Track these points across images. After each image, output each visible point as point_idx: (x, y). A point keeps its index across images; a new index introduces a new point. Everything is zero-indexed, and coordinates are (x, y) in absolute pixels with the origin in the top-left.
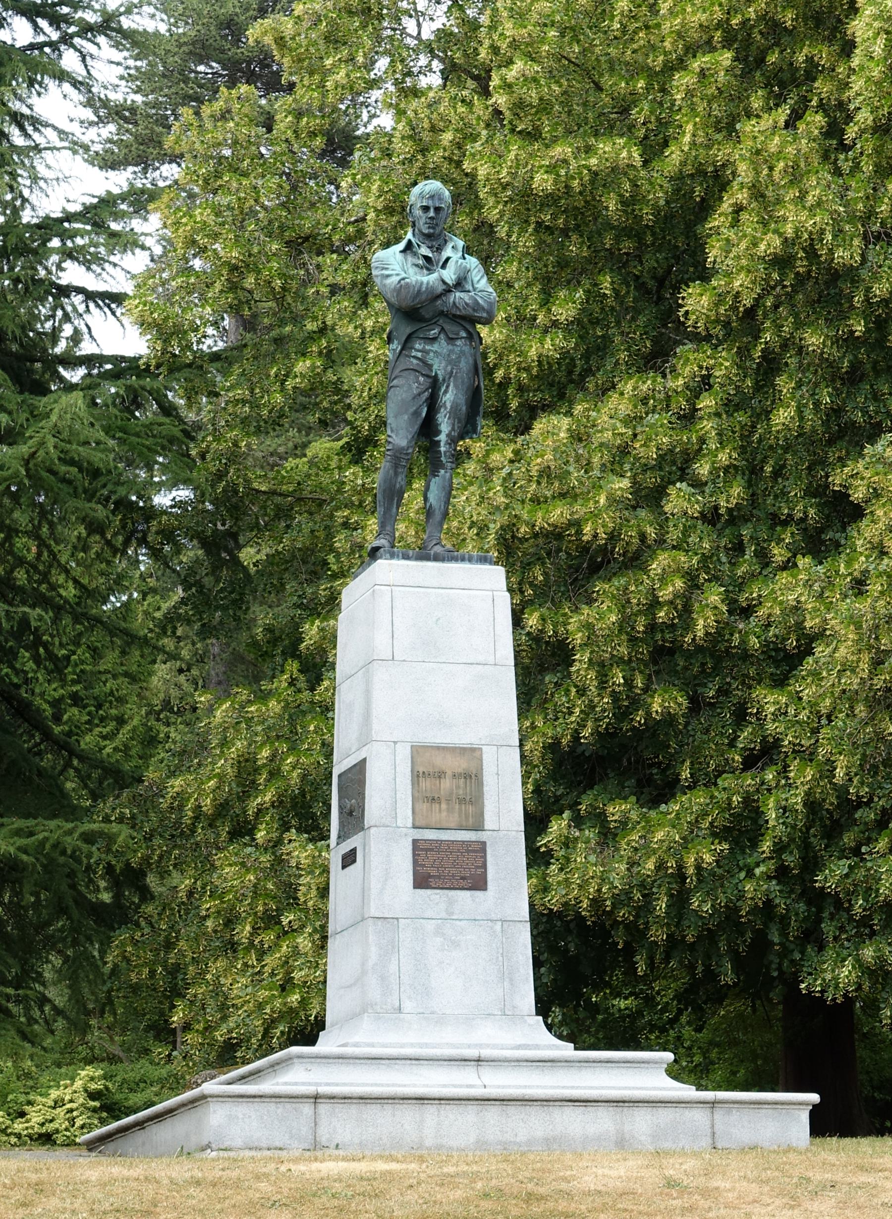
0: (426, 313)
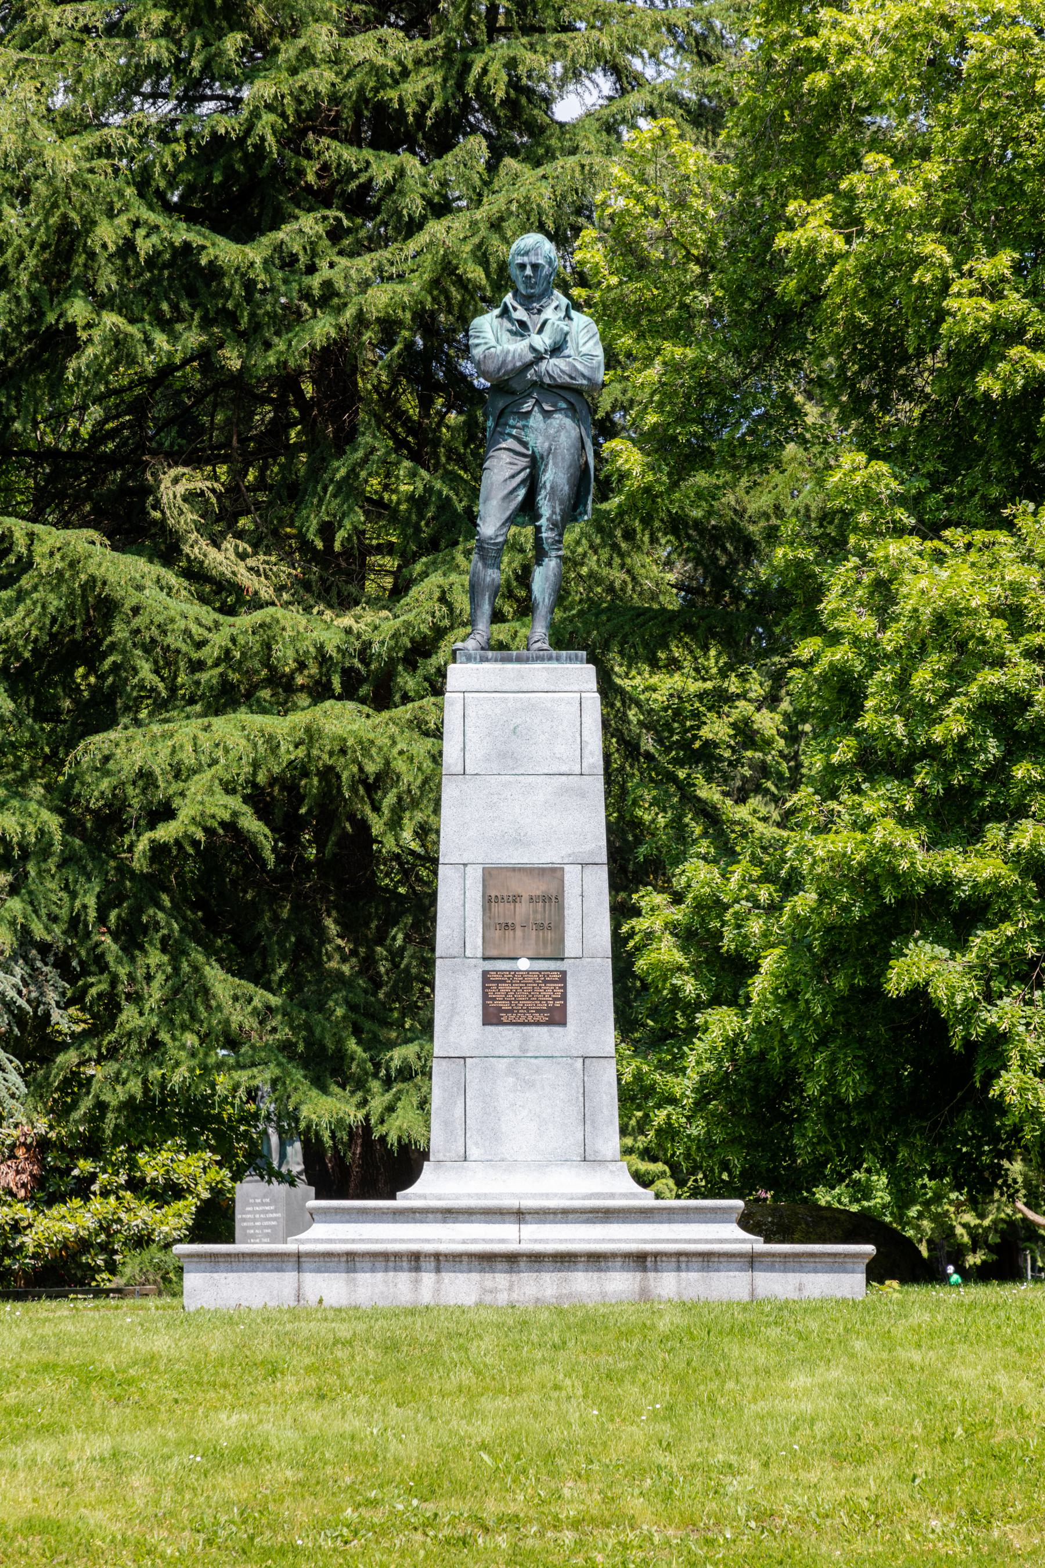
0: (515, 385)
